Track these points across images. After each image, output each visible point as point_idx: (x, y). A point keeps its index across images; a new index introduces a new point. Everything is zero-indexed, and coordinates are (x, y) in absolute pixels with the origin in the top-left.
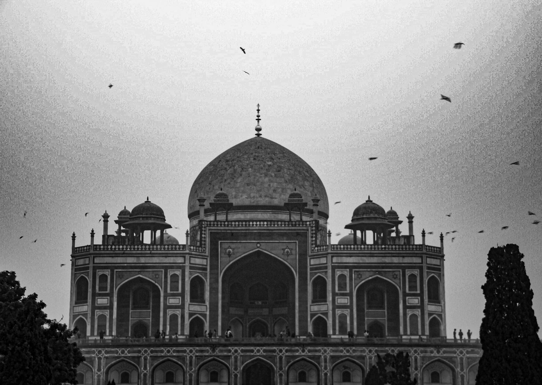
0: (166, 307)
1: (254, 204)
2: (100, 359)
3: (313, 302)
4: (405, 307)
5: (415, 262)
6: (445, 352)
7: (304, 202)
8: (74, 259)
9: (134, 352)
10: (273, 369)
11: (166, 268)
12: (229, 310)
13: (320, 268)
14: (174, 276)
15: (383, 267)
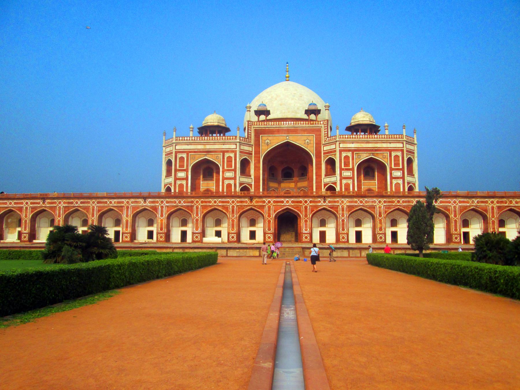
0: (224, 179)
1: (285, 117)
2: (162, 207)
3: (326, 176)
4: (392, 178)
5: (398, 146)
6: (441, 202)
7: (319, 108)
8: (164, 148)
9: (189, 202)
10: (300, 216)
11: (224, 152)
12: (268, 184)
13: (331, 152)
14: (229, 158)
15: (376, 150)
